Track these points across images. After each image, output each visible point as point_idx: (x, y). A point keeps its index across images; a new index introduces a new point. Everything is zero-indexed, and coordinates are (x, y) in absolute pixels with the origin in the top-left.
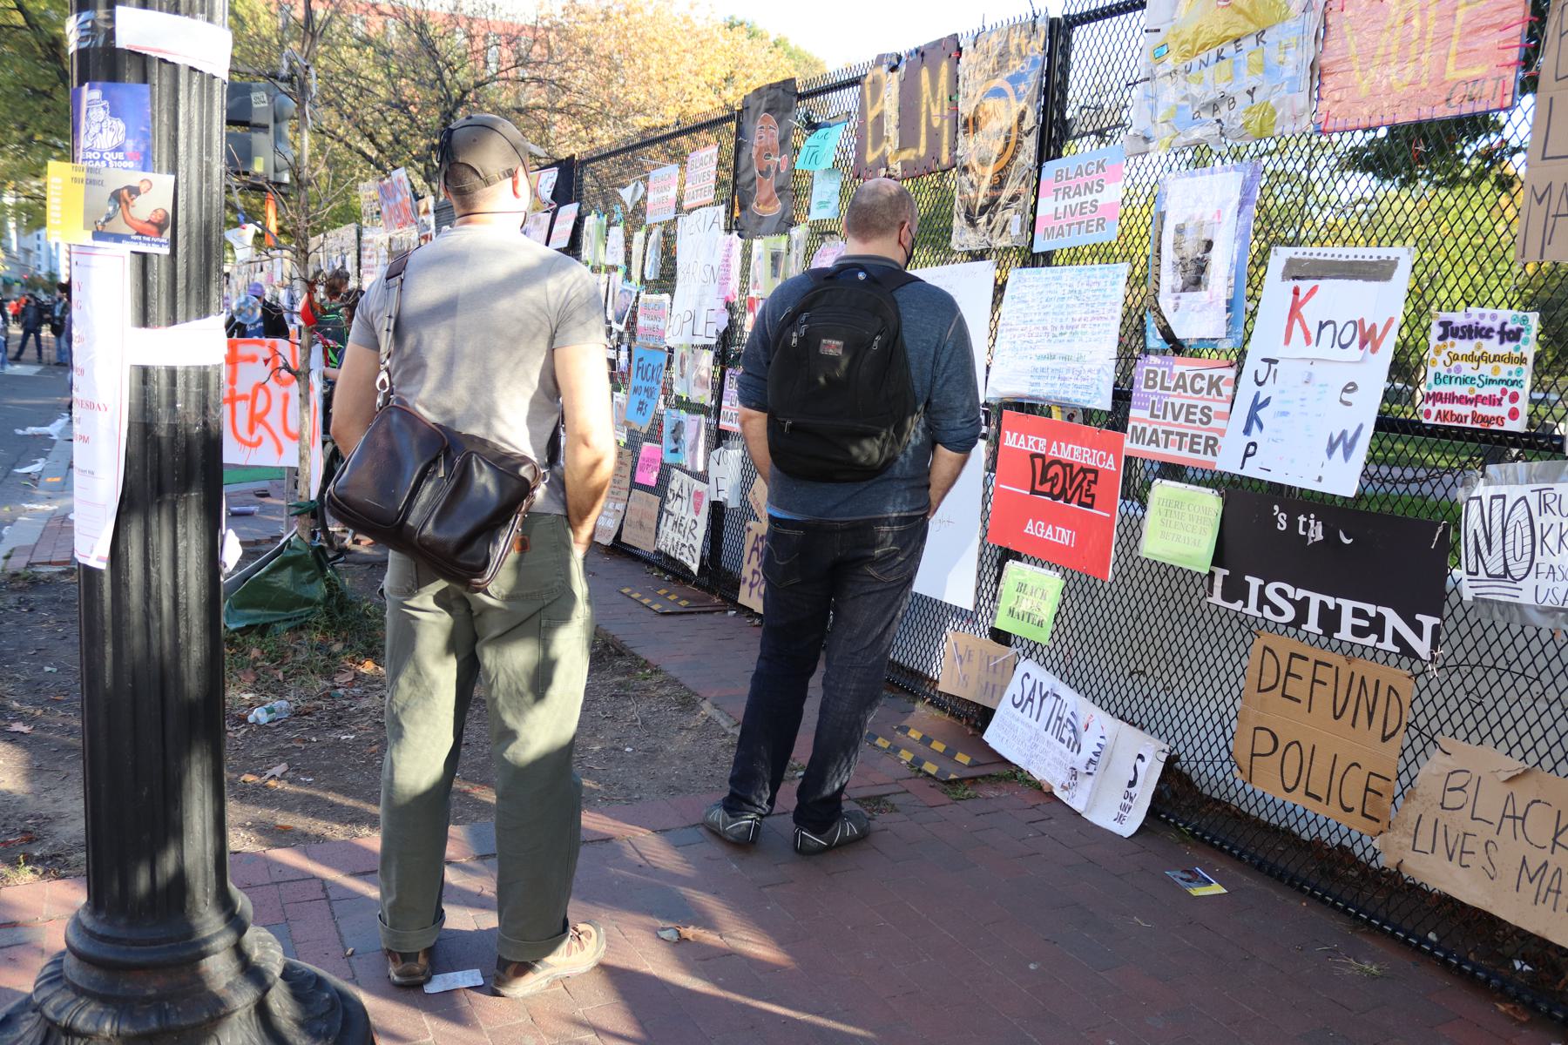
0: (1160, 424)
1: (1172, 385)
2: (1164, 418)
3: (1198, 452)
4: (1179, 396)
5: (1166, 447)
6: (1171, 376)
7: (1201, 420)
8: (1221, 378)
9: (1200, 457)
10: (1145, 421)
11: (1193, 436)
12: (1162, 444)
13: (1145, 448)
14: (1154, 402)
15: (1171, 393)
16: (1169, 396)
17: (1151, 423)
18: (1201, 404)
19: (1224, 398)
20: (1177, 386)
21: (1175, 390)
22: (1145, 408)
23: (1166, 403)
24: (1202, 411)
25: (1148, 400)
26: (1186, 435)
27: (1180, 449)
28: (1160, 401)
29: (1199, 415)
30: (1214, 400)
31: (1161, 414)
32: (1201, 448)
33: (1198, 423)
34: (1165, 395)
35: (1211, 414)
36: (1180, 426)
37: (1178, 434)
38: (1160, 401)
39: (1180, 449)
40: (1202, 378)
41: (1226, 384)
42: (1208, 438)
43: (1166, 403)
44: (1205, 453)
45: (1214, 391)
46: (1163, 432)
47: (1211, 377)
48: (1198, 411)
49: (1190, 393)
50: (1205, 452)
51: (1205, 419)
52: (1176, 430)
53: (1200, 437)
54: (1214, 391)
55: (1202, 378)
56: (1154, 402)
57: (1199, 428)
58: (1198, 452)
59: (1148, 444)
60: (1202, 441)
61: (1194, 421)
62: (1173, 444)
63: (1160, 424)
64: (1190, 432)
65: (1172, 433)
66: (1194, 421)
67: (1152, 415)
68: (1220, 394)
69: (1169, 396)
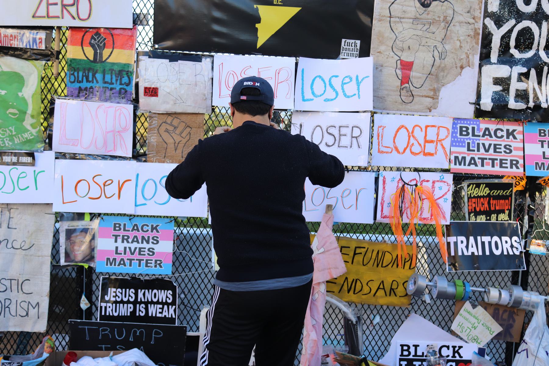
0: (476, 154)
1: (481, 134)
2: (478, 150)
3: (507, 167)
4: (487, 139)
5: (483, 165)
6: (479, 129)
7: (505, 152)
8: (514, 131)
9: (509, 170)
10: (464, 153)
11: (501, 160)
12: (479, 165)
13: (467, 167)
14: (469, 144)
15: (481, 138)
16: (479, 140)
17: (468, 155)
18: (503, 144)
19: (518, 140)
20: (484, 135)
21: (483, 136)
22: (464, 147)
23: (478, 144)
24: (505, 147)
25: (465, 142)
26: (497, 159)
27: (493, 166)
28: (473, 142)
29: (503, 149)
30: (512, 141)
31: (476, 149)
32: (508, 165)
33: (503, 153)
34: (476, 140)
35: (512, 148)
36: (491, 155)
37: (490, 159)
38: (473, 142)
39: (493, 166)
40: (502, 130)
41: (518, 133)
42: (511, 161)
43: (478, 144)
44: (511, 167)
45: (511, 137)
46: (479, 158)
47: (508, 130)
48: (502, 147)
49: (494, 138)
50: (511, 167)
51: (508, 151)
52: (488, 157)
53: (507, 160)
54: (511, 137)
55: (502, 130)
56: (469, 144)
57: (504, 156)
58: (507, 167)
59: (469, 165)
60: (509, 162)
61: (501, 152)
62: (488, 164)
63: (476, 154)
64: (499, 158)
65: (486, 159)
66: (501, 152)
67: (469, 149)
68: (515, 138)
69: (479, 140)
